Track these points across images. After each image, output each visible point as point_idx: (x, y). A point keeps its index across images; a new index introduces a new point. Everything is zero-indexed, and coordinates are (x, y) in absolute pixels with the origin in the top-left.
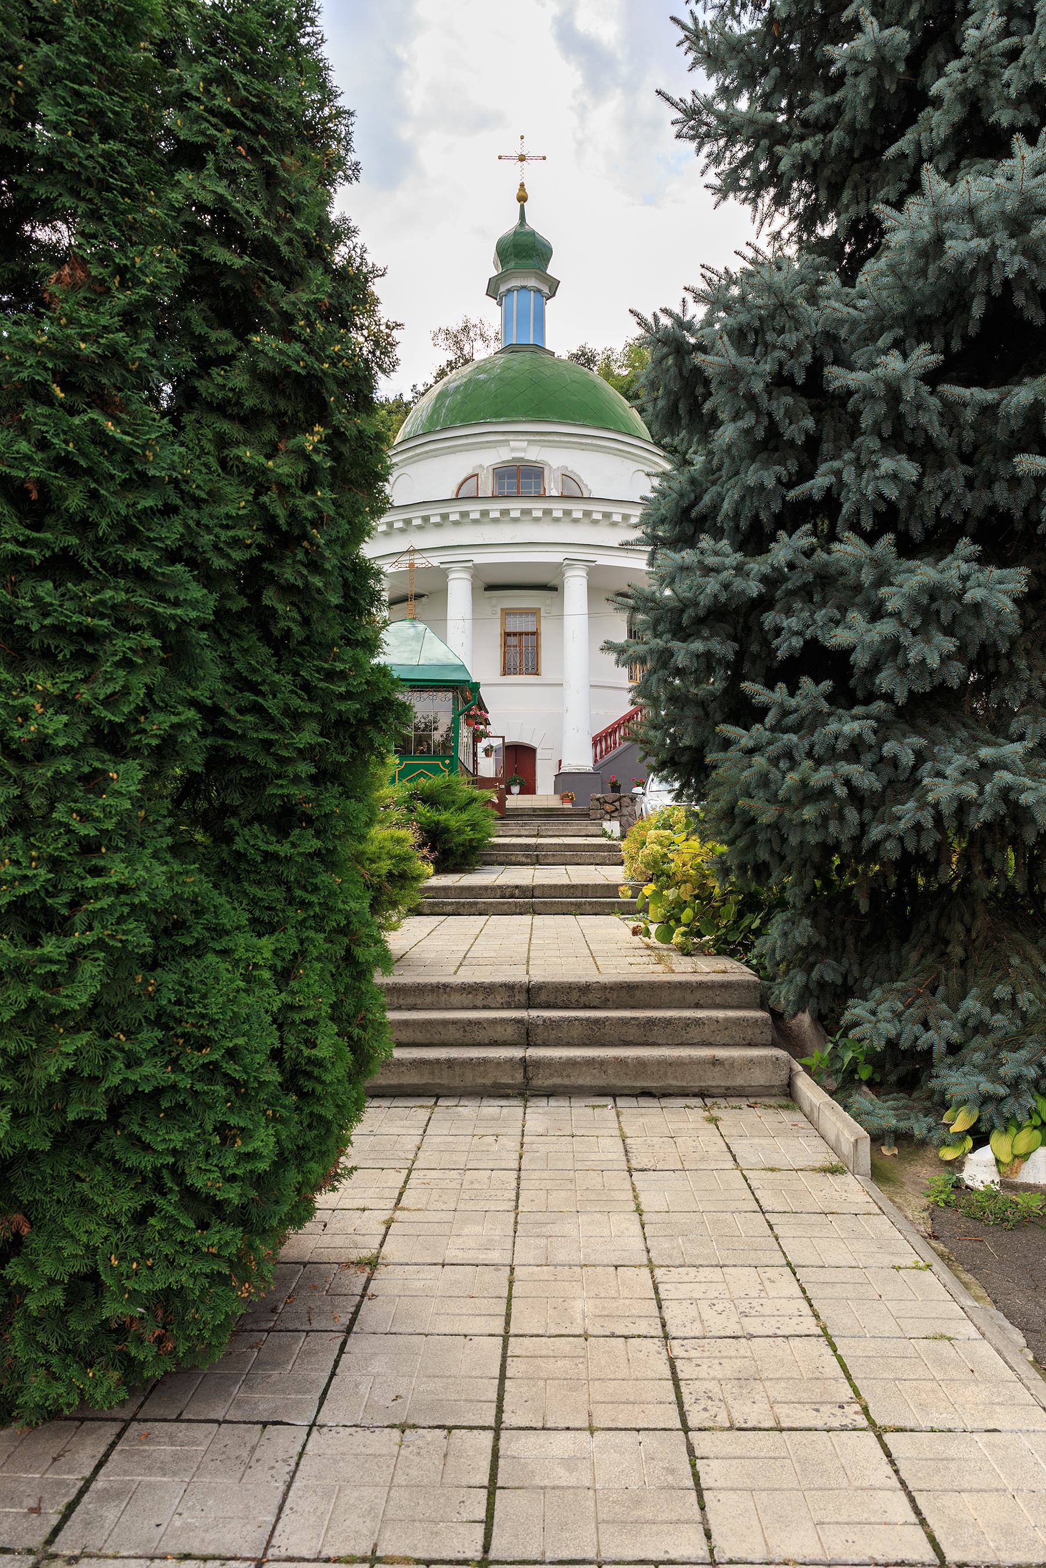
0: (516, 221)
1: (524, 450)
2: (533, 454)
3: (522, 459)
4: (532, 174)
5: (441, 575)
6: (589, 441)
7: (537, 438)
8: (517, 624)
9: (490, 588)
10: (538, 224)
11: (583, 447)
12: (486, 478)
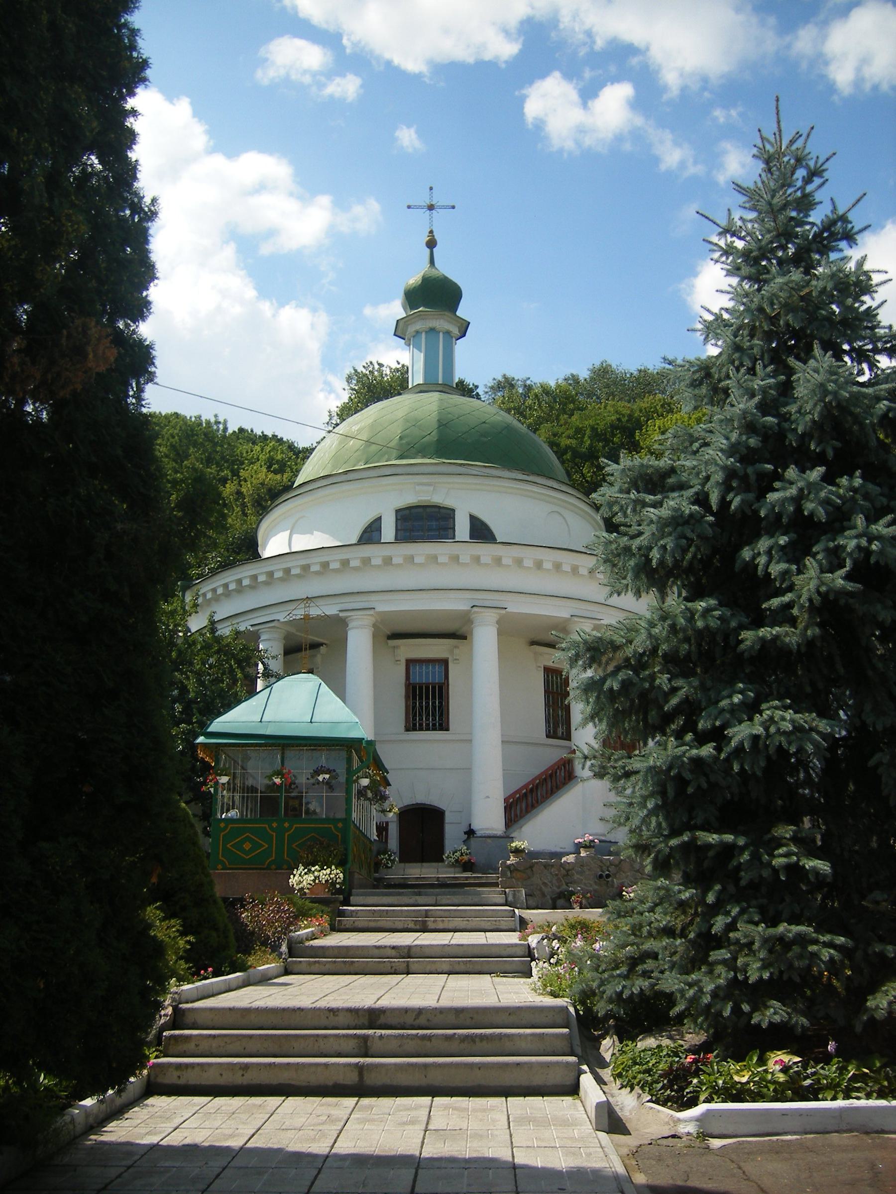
2: (439, 497)
4: (441, 223)
8: (423, 676)
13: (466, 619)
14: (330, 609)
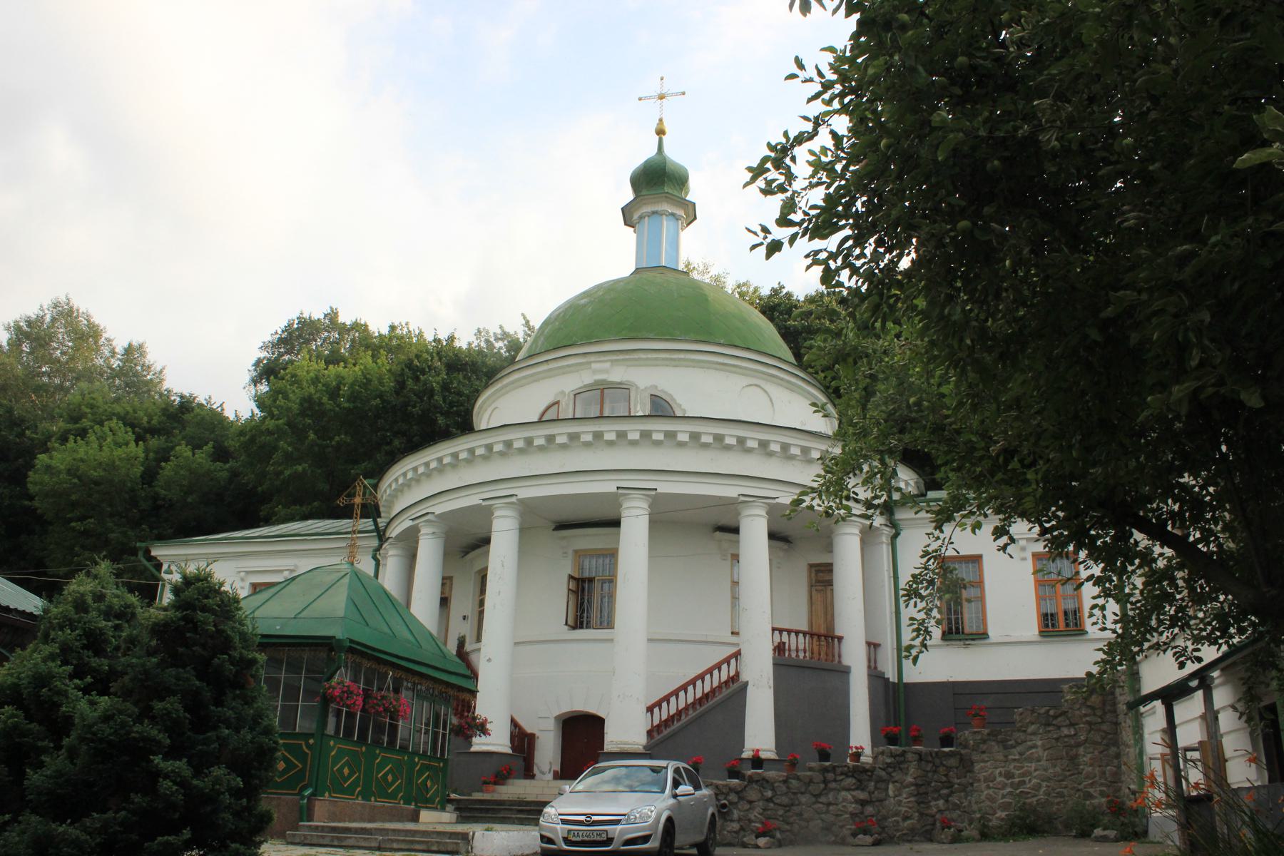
0: (655, 151)
1: (607, 371)
2: (617, 374)
3: (603, 382)
5: (484, 513)
6: (682, 356)
7: (621, 357)
8: (591, 568)
9: (562, 526)
10: (676, 154)
11: (676, 364)
12: (567, 405)
13: (614, 499)
14: (472, 499)
